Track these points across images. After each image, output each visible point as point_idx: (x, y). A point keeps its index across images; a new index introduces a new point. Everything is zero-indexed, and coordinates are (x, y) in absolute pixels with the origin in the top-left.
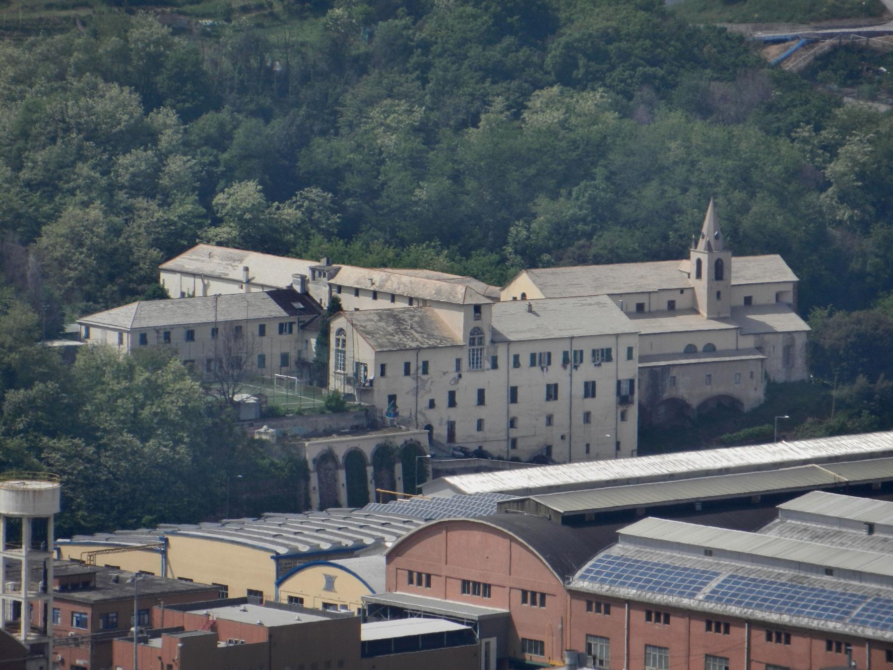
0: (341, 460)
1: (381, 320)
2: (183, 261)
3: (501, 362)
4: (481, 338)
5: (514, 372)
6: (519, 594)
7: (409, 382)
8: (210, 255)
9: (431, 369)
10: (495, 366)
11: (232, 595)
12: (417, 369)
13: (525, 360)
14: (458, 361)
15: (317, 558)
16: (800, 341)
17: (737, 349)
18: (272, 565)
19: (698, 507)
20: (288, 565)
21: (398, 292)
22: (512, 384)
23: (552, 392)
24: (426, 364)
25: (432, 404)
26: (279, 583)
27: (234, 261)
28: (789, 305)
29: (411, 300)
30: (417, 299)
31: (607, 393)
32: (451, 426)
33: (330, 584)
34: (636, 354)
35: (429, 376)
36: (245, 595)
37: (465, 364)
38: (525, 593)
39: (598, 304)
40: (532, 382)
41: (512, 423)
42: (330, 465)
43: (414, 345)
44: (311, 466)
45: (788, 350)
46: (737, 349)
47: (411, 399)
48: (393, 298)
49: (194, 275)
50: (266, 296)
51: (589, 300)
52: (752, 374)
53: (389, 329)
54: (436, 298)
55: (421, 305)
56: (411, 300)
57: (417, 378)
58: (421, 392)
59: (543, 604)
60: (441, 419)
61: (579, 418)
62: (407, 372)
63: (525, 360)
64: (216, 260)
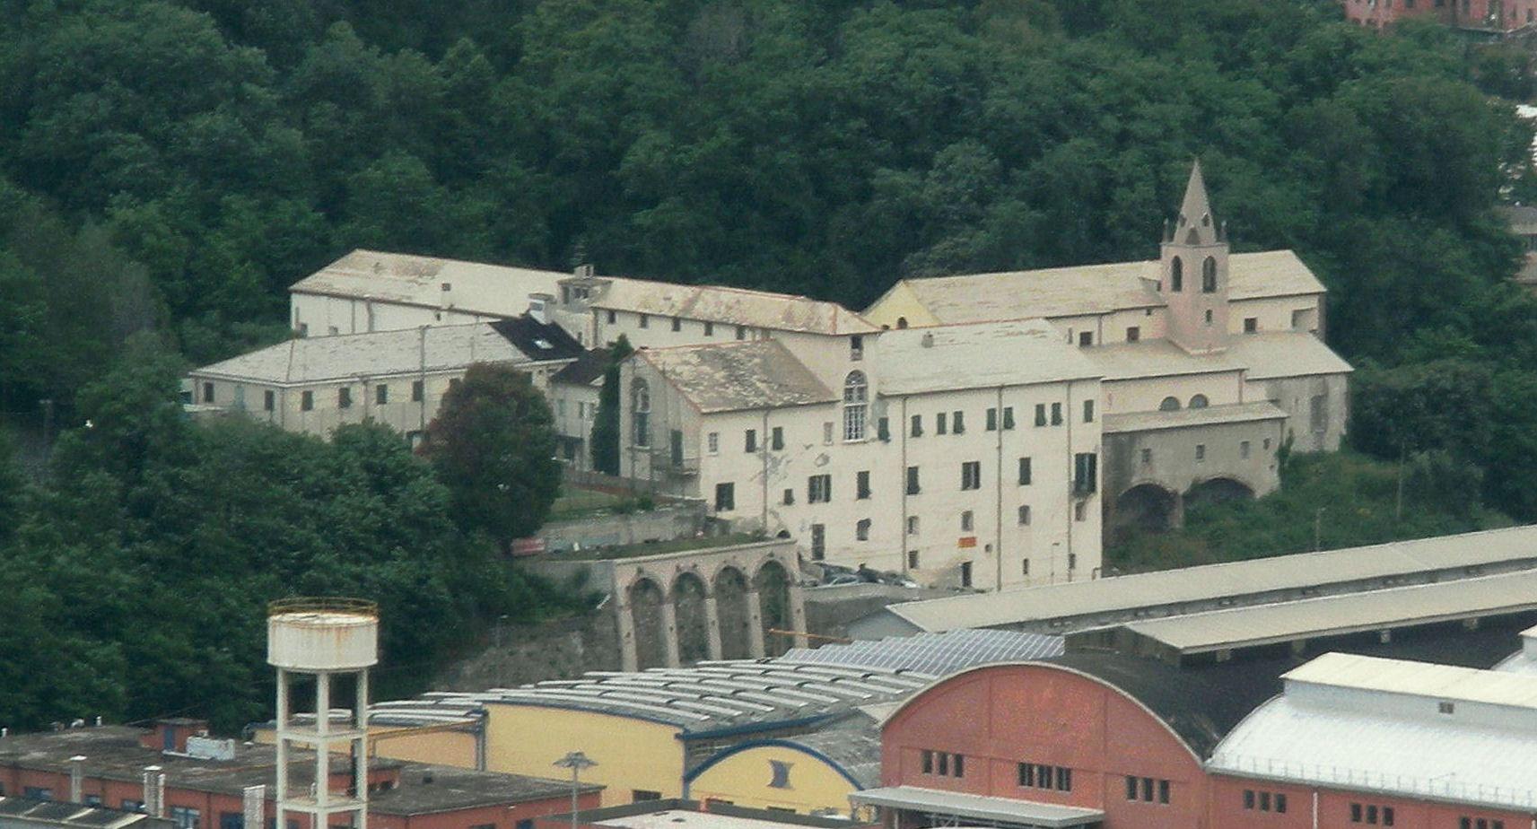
0: (710, 587)
1: (703, 361)
2: (331, 277)
3: (894, 428)
4: (861, 390)
5: (913, 443)
6: (1122, 784)
7: (753, 463)
8: (378, 267)
9: (787, 438)
10: (884, 435)
11: (607, 802)
12: (766, 440)
13: (929, 425)
14: (829, 426)
15: (744, 736)
16: (1338, 389)
17: (1241, 403)
18: (678, 751)
19: (1385, 638)
20: (707, 746)
21: (717, 317)
22: (911, 464)
23: (971, 476)
24: (778, 432)
25: (789, 499)
26: (689, 777)
27: (421, 275)
28: (1313, 331)
29: (741, 330)
30: (753, 328)
31: (1054, 477)
32: (818, 531)
33: (781, 776)
34: (1097, 412)
35: (783, 452)
36: (630, 801)
37: (839, 430)
38: (1132, 782)
39: (1032, 332)
40: (939, 459)
41: (911, 523)
42: (650, 596)
43: (760, 401)
44: (622, 599)
45: (1318, 403)
46: (1241, 403)
47: (756, 488)
48: (709, 326)
49: (352, 299)
50: (490, 329)
51: (1018, 327)
52: (1267, 442)
53: (717, 376)
54: (782, 324)
55: (758, 337)
56: (741, 330)
57: (765, 457)
58: (772, 479)
59: (1165, 799)
60: (803, 522)
61: (1011, 516)
62: (750, 447)
63: (929, 425)
64: (388, 275)
